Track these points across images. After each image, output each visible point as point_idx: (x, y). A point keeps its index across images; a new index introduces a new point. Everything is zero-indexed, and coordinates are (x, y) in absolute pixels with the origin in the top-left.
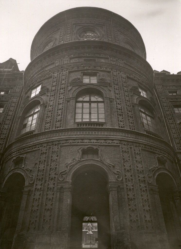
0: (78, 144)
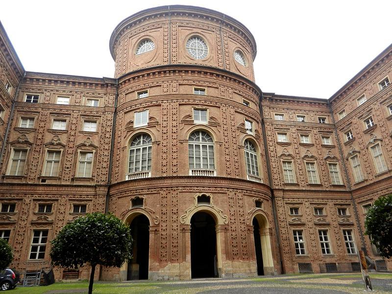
0: (194, 191)
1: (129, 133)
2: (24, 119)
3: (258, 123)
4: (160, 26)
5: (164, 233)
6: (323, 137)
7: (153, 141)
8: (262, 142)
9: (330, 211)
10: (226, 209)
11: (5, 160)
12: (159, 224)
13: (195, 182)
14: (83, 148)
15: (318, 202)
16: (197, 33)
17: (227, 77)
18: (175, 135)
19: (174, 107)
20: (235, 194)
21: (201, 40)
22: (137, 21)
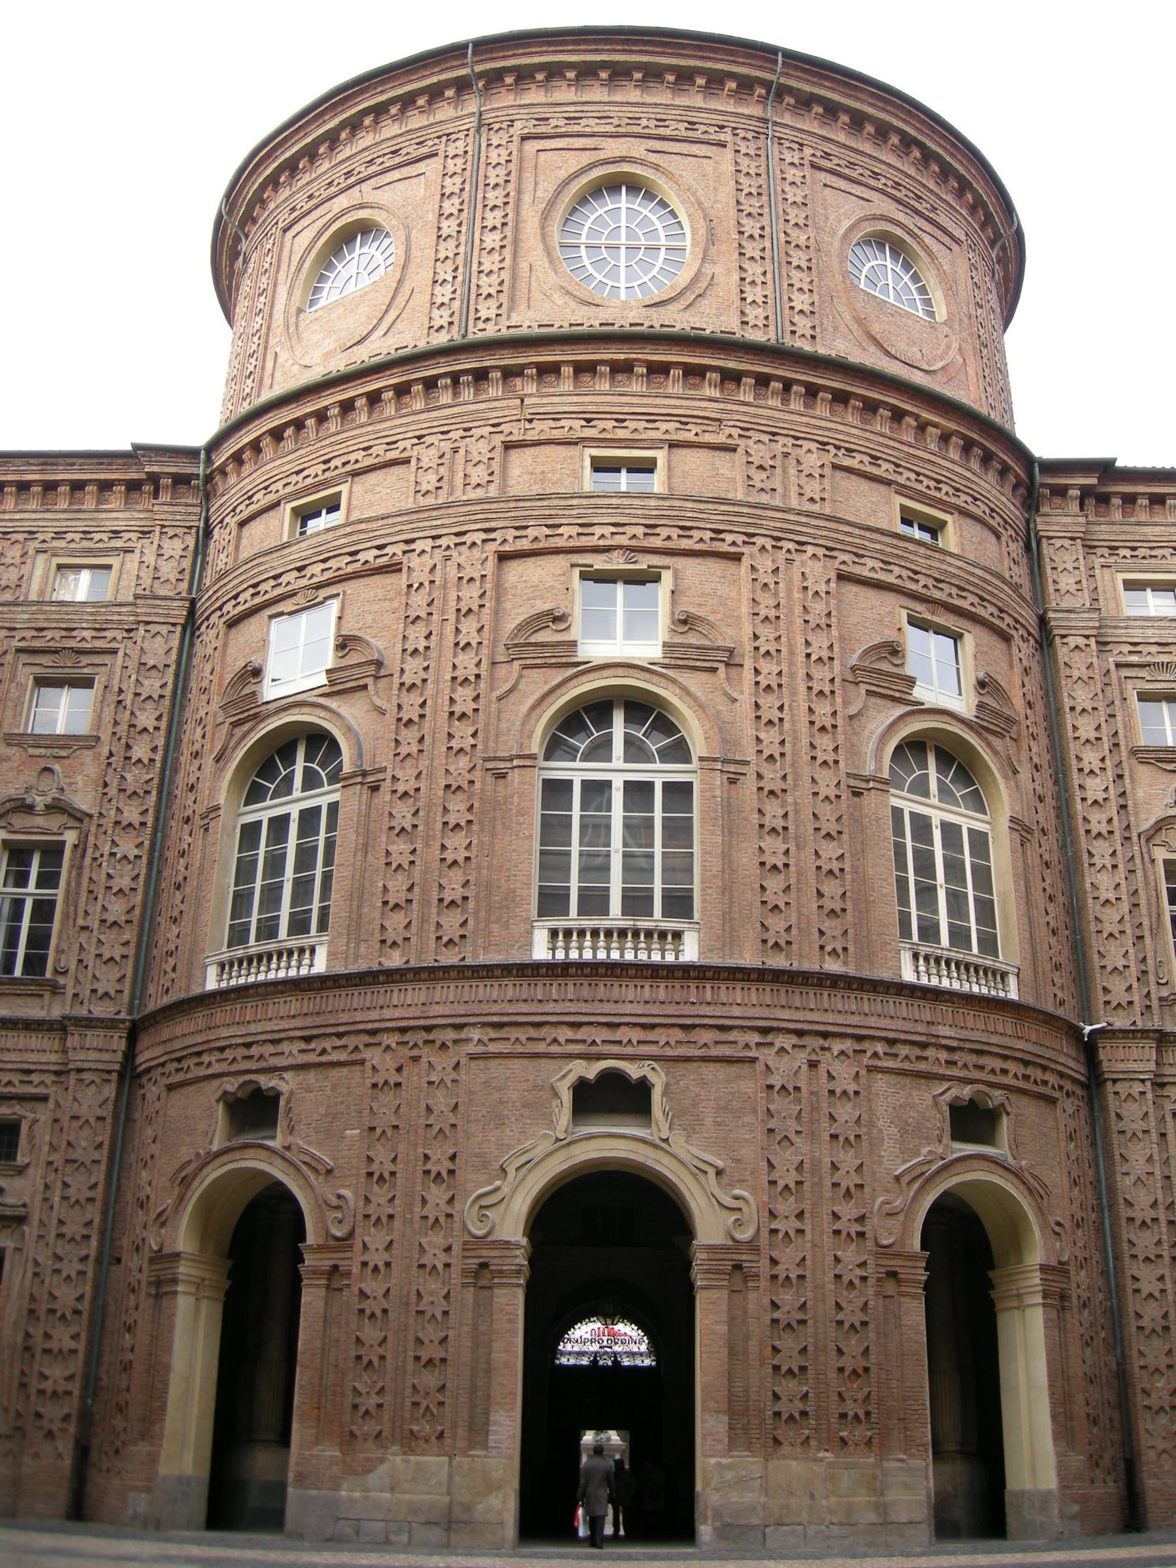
0: (554, 1049)
1: (239, 732)
3: (1006, 638)
4: (424, 150)
5: (374, 1286)
8: (1039, 750)
10: (747, 1153)
12: (351, 1234)
13: (562, 998)
14: (18, 821)
16: (623, 159)
17: (788, 385)
18: (463, 730)
19: (467, 573)
20: (813, 1065)
21: (650, 196)
22: (317, 143)
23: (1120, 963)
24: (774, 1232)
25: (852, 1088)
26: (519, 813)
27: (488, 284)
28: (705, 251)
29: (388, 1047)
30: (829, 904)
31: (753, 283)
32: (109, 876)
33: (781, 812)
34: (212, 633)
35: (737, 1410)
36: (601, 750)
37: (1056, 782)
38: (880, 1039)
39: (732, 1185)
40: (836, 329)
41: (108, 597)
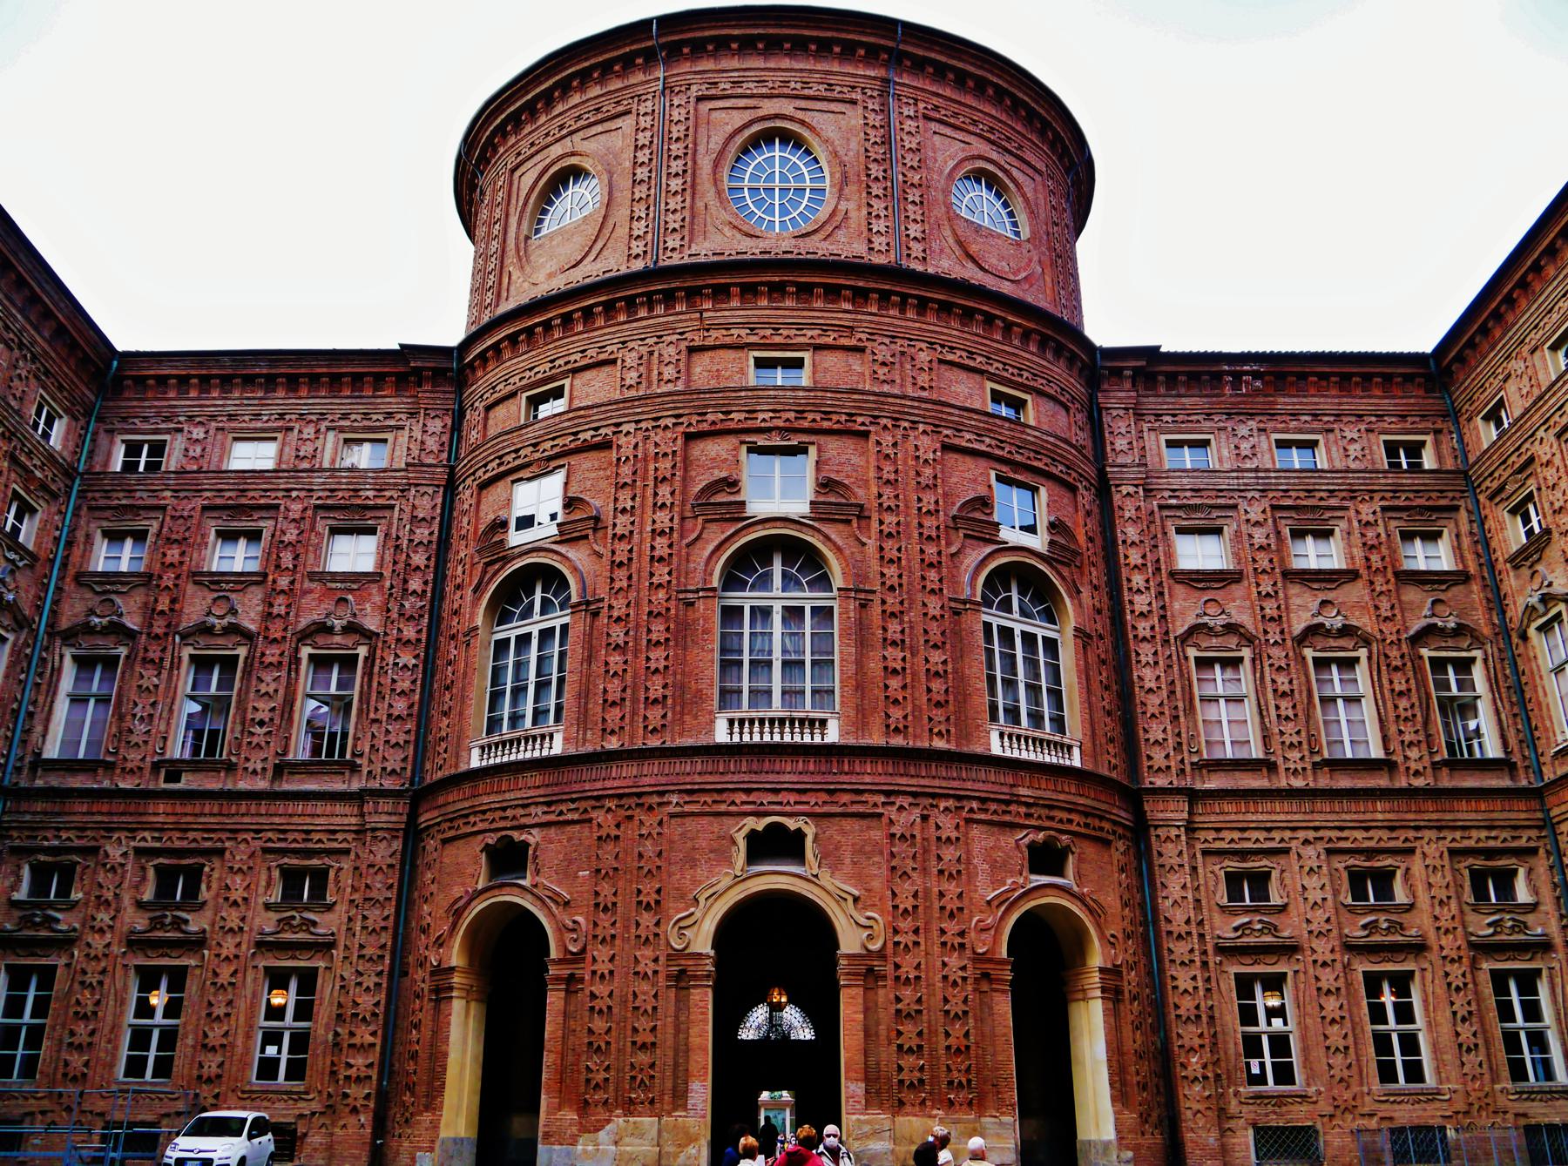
1: (491, 570)
2: (115, 537)
3: (1073, 489)
4: (621, 108)
5: (601, 989)
6: (1408, 536)
7: (574, 599)
8: (1096, 574)
9: (1425, 887)
11: (41, 699)
12: (583, 950)
13: (738, 773)
14: (320, 640)
15: (1367, 844)
16: (777, 116)
17: (904, 297)
19: (663, 448)
20: (925, 818)
21: (798, 146)
23: (1160, 737)
24: (897, 944)
25: (954, 835)
26: (704, 632)
27: (674, 221)
28: (841, 190)
29: (609, 809)
30: (936, 697)
31: (878, 217)
32: (394, 681)
33: (899, 628)
34: (468, 493)
35: (871, 1078)
36: (764, 582)
37: (1111, 598)
38: (974, 798)
39: (865, 908)
40: (942, 251)
41: (384, 464)
